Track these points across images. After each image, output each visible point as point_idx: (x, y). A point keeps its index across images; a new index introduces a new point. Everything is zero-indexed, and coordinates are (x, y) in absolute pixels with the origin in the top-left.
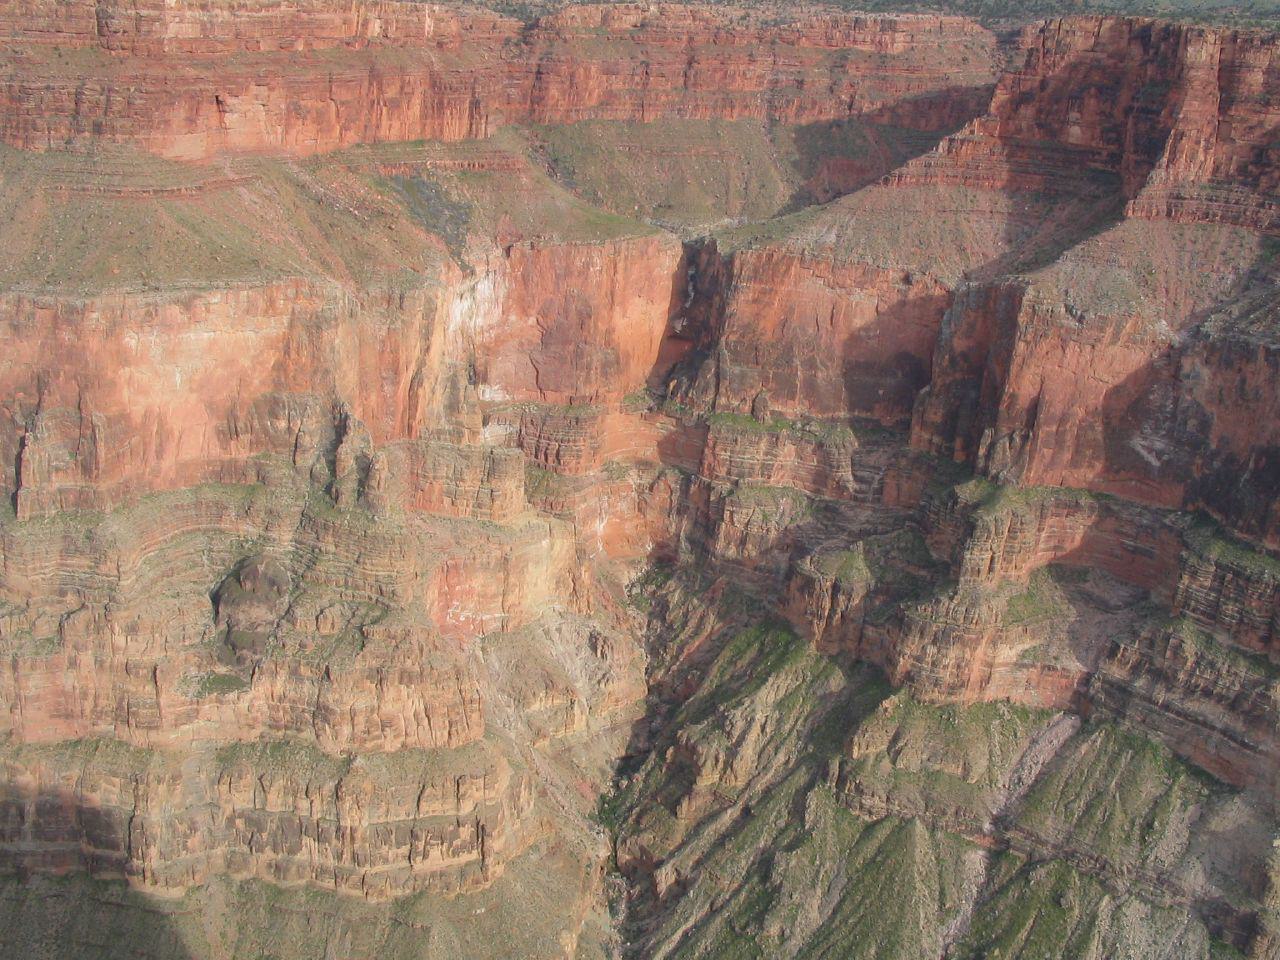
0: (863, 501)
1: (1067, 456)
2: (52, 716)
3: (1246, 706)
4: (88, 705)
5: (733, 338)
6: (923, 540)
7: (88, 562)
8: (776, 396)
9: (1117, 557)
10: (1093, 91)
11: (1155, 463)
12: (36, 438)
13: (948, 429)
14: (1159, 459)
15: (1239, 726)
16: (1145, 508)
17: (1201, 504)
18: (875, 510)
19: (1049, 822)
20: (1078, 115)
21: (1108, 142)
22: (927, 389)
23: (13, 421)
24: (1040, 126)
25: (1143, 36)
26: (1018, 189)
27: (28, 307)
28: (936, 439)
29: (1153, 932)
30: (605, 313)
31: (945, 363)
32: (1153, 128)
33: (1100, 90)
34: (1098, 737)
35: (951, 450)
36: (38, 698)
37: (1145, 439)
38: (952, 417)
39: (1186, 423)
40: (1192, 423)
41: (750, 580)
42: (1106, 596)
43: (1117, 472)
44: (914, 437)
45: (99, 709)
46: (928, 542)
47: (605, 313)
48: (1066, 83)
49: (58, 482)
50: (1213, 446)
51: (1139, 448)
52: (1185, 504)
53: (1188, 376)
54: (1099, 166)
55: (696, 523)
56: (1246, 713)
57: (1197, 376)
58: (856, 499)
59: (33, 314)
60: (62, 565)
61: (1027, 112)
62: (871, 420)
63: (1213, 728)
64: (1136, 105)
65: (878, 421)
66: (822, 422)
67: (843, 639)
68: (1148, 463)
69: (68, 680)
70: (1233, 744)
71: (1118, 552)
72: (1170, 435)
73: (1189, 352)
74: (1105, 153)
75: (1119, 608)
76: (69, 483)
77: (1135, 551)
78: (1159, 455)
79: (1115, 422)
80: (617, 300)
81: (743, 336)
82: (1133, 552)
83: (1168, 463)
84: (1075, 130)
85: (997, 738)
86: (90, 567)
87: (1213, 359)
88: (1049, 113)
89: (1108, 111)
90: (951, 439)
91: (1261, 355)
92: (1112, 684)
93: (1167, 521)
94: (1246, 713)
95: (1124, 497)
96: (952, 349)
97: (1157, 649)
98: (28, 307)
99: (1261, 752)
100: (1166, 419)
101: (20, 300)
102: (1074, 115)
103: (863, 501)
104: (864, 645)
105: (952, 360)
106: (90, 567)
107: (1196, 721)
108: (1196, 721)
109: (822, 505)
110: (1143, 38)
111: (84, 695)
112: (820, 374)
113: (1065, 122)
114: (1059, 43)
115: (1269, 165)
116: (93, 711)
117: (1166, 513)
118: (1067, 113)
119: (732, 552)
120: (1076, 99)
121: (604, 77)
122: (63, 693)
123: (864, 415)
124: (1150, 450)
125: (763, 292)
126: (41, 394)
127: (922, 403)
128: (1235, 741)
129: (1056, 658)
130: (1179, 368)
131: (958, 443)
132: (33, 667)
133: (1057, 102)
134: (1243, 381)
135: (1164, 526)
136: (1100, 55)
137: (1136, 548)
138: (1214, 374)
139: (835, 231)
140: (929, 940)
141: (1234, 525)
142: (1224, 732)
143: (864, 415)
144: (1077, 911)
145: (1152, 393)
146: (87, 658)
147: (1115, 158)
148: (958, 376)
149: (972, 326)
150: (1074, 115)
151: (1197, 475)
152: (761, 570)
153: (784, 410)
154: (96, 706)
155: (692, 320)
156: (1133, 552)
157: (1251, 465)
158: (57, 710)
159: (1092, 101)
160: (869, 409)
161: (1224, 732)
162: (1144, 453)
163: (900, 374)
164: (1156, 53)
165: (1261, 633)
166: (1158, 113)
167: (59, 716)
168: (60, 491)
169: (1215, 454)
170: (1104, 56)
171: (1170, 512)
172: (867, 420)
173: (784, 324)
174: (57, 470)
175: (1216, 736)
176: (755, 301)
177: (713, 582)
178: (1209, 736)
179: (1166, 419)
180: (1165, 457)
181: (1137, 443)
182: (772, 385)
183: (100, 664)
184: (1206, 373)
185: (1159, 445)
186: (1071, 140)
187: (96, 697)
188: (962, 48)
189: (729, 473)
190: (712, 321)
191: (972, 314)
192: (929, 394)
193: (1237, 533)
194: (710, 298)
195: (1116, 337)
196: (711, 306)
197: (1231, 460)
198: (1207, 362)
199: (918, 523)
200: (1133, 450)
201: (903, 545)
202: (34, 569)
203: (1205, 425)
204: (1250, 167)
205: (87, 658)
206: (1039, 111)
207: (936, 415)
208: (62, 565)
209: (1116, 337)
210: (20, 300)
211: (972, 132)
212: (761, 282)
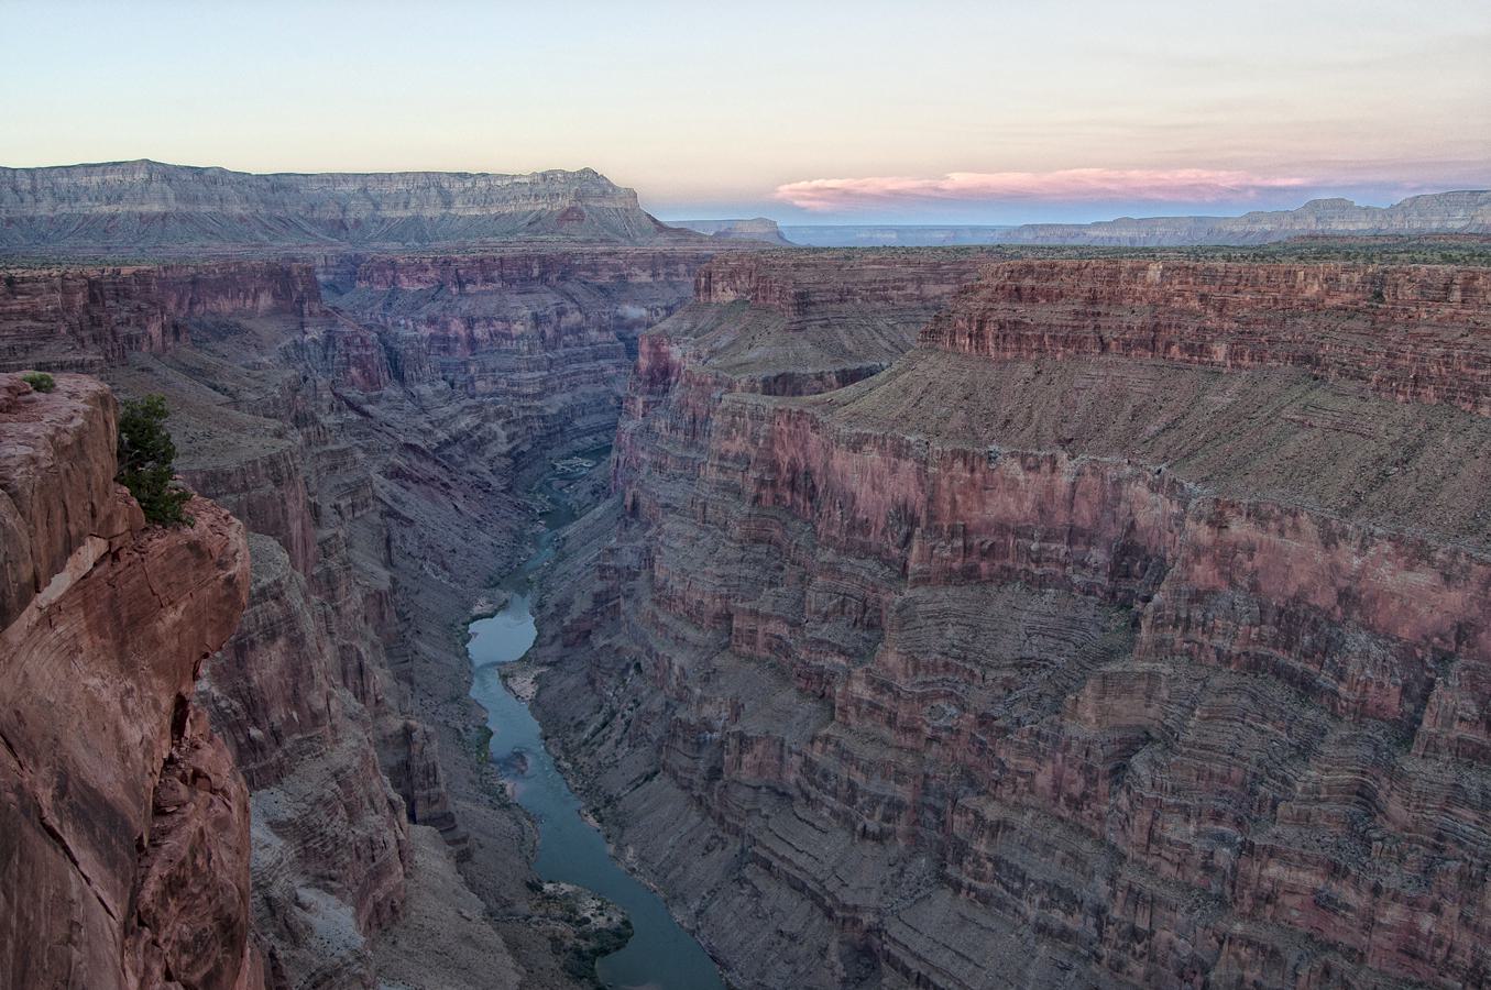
2: (1399, 950)
4: (1440, 953)
7: (1476, 817)
12: (1446, 684)
23: (1422, 661)
27: (1463, 561)
36: (1390, 928)
45: (1450, 962)
49: (1459, 730)
59: (1468, 569)
60: (1446, 811)
69: (1426, 923)
76: (1470, 736)
86: (1477, 823)
98: (1463, 561)
101: (1456, 553)
106: (1477, 823)
111: (1439, 944)
116: (1444, 961)
122: (1417, 934)
126: (1459, 643)
132: (1395, 898)
146: (1451, 910)
154: (1448, 957)
158: (1406, 946)
167: (1407, 953)
168: (1459, 740)
174: (1462, 719)
183: (1465, 921)
187: (1451, 949)
202: (1418, 807)
205: (1451, 910)
208: (1446, 811)
210: (1456, 553)
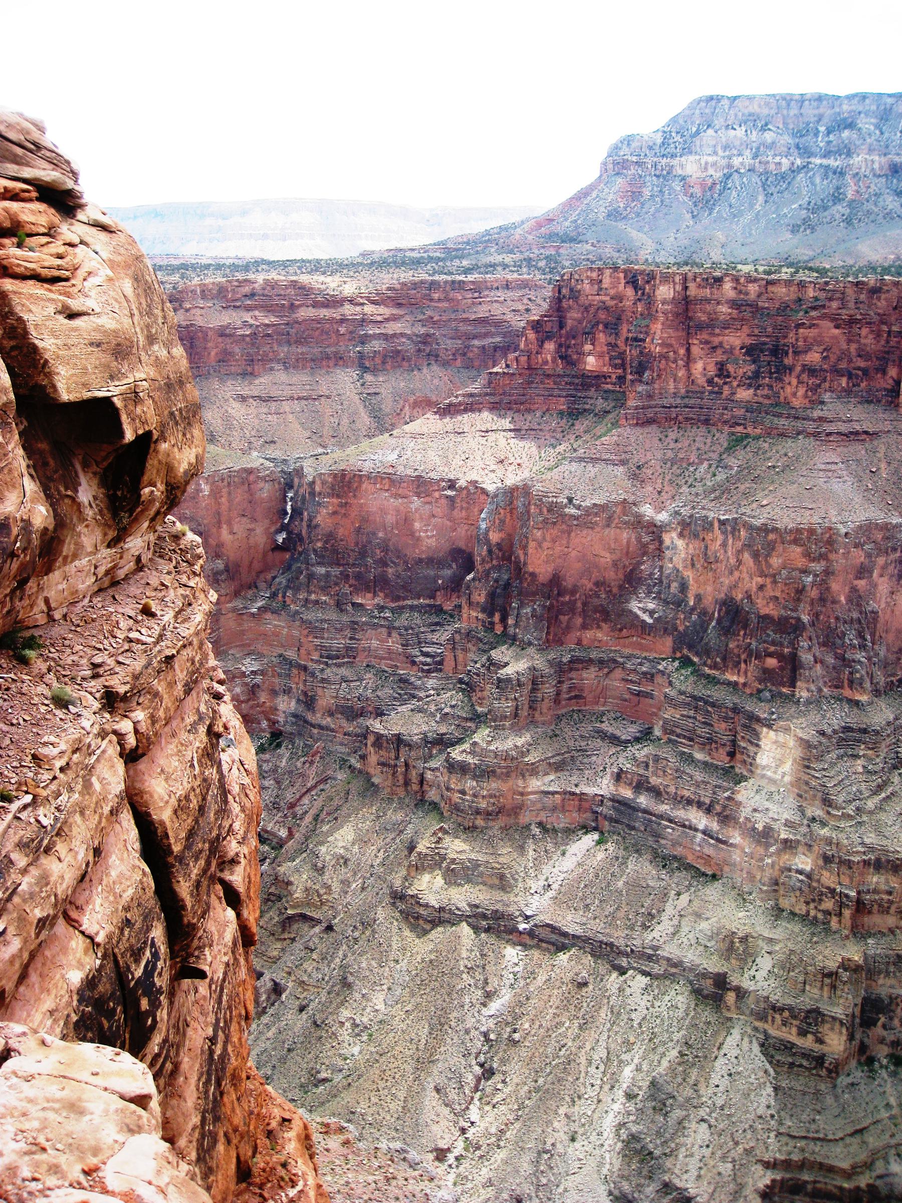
0: (429, 671)
1: (579, 621)
3: (718, 808)
5: (319, 544)
6: (470, 698)
8: (356, 590)
9: (626, 700)
10: (601, 327)
11: (650, 621)
13: (489, 608)
14: (651, 617)
15: (715, 826)
16: (645, 658)
17: (685, 651)
18: (439, 679)
19: (569, 918)
20: (591, 347)
21: (615, 366)
22: (471, 576)
24: (561, 357)
25: (632, 280)
26: (548, 410)
28: (480, 616)
29: (650, 998)
30: (214, 530)
31: (484, 553)
32: (641, 352)
33: (606, 326)
34: (610, 846)
35: (492, 624)
37: (640, 602)
38: (492, 596)
39: (669, 587)
40: (674, 585)
41: (341, 744)
42: (618, 733)
43: (621, 630)
44: (465, 615)
46: (474, 699)
47: (214, 530)
48: (580, 322)
50: (692, 603)
51: (636, 610)
52: (674, 652)
53: (668, 548)
54: (610, 387)
55: (298, 701)
56: (718, 814)
57: (675, 548)
58: (423, 671)
61: (550, 346)
62: (434, 606)
63: (696, 830)
64: (630, 335)
65: (440, 605)
66: (393, 611)
67: (407, 783)
68: (643, 621)
70: (712, 841)
71: (627, 697)
72: (658, 597)
73: (668, 528)
74: (614, 376)
75: (628, 741)
77: (639, 694)
78: (651, 613)
79: (615, 590)
80: (223, 519)
81: (326, 542)
82: (638, 695)
83: (657, 620)
84: (591, 360)
85: (531, 853)
87: (686, 533)
88: (569, 347)
89: (613, 342)
90: (491, 615)
91: (716, 525)
92: (618, 802)
93: (660, 667)
94: (718, 814)
95: (627, 651)
96: (488, 541)
97: (651, 769)
99: (732, 845)
100: (656, 584)
102: (588, 347)
103: (429, 671)
104: (425, 787)
105: (490, 552)
107: (684, 826)
108: (684, 826)
109: (396, 678)
110: (633, 282)
112: (390, 570)
113: (582, 354)
114: (571, 290)
115: (729, 377)
117: (658, 661)
118: (582, 345)
119: (328, 721)
120: (590, 335)
121: (220, 340)
123: (427, 602)
124: (645, 610)
125: (341, 505)
127: (468, 588)
128: (712, 838)
129: (576, 786)
130: (661, 542)
131: (497, 617)
133: (574, 338)
134: (706, 547)
135: (660, 671)
136: (604, 298)
137: (640, 692)
138: (687, 544)
139: (397, 452)
140: (474, 1020)
141: (705, 664)
142: (704, 832)
143: (427, 602)
144: (591, 987)
145: (642, 563)
147: (621, 379)
148: (495, 562)
149: (502, 522)
150: (588, 347)
151: (681, 628)
152: (349, 735)
153: (363, 602)
155: (289, 533)
156: (638, 695)
157: (716, 615)
159: (601, 335)
160: (433, 597)
161: (704, 832)
162: (639, 613)
163: (454, 566)
164: (643, 294)
165: (728, 749)
166: (644, 341)
169: (693, 609)
170: (608, 298)
171: (663, 659)
172: (429, 605)
173: (358, 530)
175: (700, 835)
176: (335, 513)
177: (310, 747)
178: (694, 837)
179: (656, 584)
180: (656, 615)
181: (635, 606)
182: (352, 582)
184: (680, 543)
185: (651, 606)
186: (588, 368)
188: (525, 301)
189: (321, 656)
190: (304, 532)
191: (502, 511)
192: (473, 579)
193: (707, 670)
194: (302, 514)
195: (610, 518)
196: (302, 520)
197: (704, 613)
198: (681, 535)
199: (467, 684)
200: (631, 611)
201: (454, 703)
203: (684, 587)
204: (716, 379)
206: (560, 346)
207: (480, 597)
209: (610, 518)
211: (507, 366)
212: (338, 496)
